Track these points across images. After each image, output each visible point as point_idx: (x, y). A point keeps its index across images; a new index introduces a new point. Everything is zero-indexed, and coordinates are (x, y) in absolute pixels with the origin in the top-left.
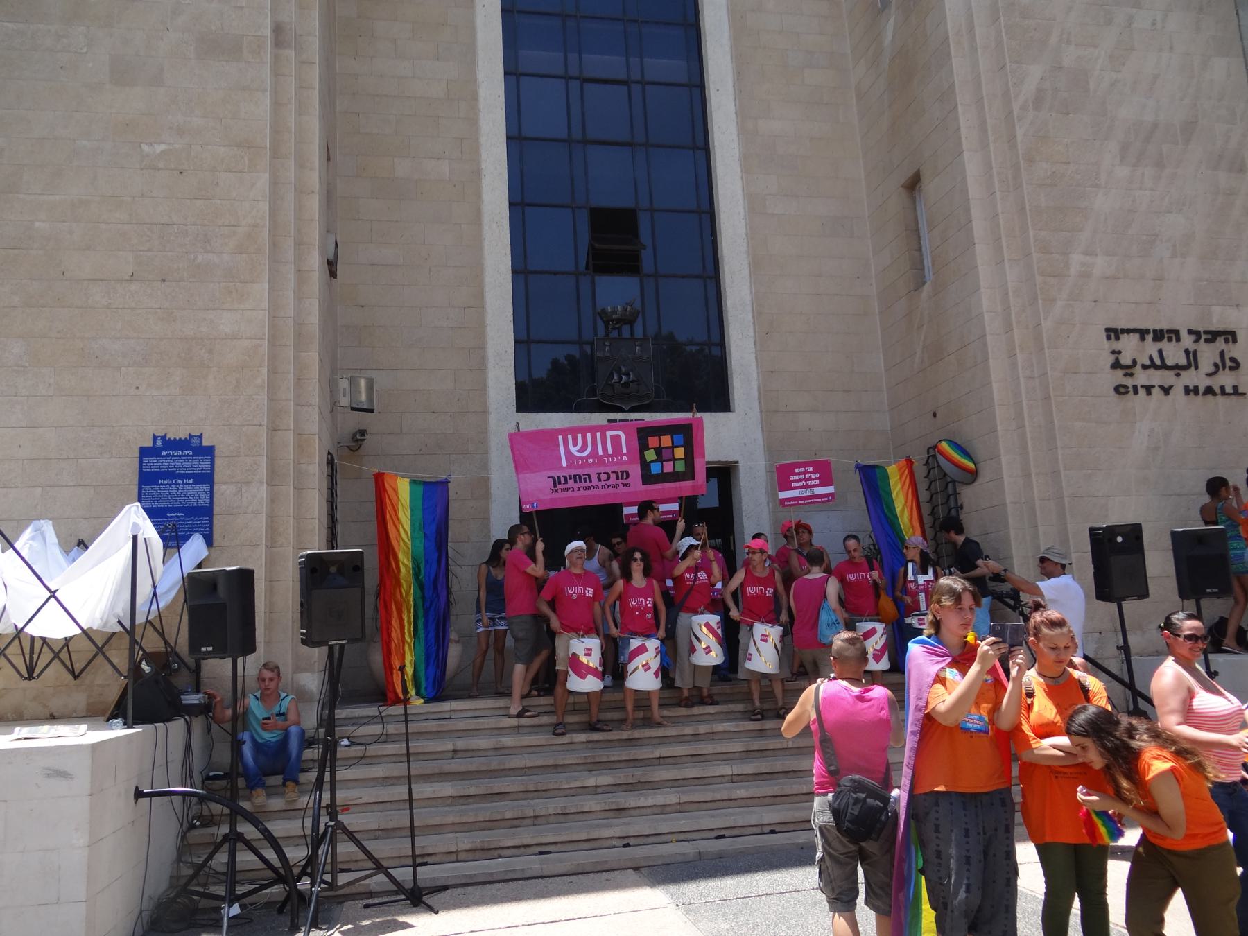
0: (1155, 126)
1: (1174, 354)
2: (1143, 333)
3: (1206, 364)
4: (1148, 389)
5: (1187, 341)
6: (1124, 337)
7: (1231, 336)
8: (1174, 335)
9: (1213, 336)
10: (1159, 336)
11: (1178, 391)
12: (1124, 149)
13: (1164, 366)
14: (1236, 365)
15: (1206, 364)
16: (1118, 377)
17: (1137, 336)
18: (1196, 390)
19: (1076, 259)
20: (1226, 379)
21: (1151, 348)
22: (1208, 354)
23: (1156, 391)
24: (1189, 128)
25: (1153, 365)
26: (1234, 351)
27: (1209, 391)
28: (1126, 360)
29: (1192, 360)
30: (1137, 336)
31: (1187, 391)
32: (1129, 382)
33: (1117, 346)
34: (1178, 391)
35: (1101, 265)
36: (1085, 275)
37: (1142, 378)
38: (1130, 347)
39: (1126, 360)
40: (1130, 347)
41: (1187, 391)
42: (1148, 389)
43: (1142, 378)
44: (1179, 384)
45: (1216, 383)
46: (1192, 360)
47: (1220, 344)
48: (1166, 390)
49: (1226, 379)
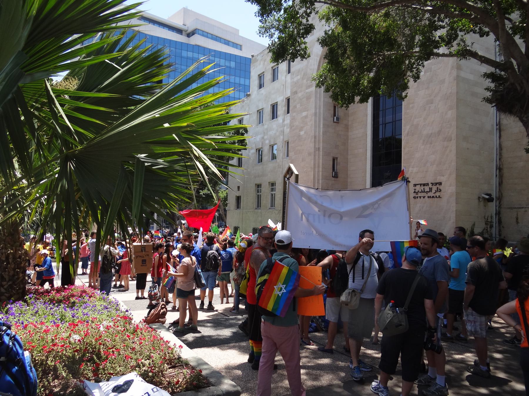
0: (432, 134)
1: (427, 189)
2: (421, 185)
3: (433, 191)
4: (420, 197)
5: (430, 186)
6: (417, 186)
7: (440, 184)
8: (428, 184)
9: (436, 184)
10: (424, 185)
11: (426, 197)
12: (424, 141)
13: (424, 192)
14: (440, 191)
15: (433, 191)
16: (415, 195)
17: (419, 186)
18: (430, 197)
19: (411, 169)
20: (438, 194)
21: (422, 188)
22: (434, 188)
23: (422, 198)
24: (439, 132)
25: (422, 192)
26: (441, 187)
27: (433, 197)
28: (417, 191)
29: (431, 189)
30: (419, 186)
31: (428, 197)
32: (417, 196)
33: (415, 188)
34: (426, 197)
35: (415, 170)
36: (411, 173)
37: (420, 195)
38: (418, 188)
39: (417, 191)
40: (418, 188)
41: (428, 197)
42: (420, 197)
43: (420, 195)
44: (426, 196)
45: (434, 195)
46: (431, 189)
47: (438, 186)
48: (424, 197)
49: (438, 194)
